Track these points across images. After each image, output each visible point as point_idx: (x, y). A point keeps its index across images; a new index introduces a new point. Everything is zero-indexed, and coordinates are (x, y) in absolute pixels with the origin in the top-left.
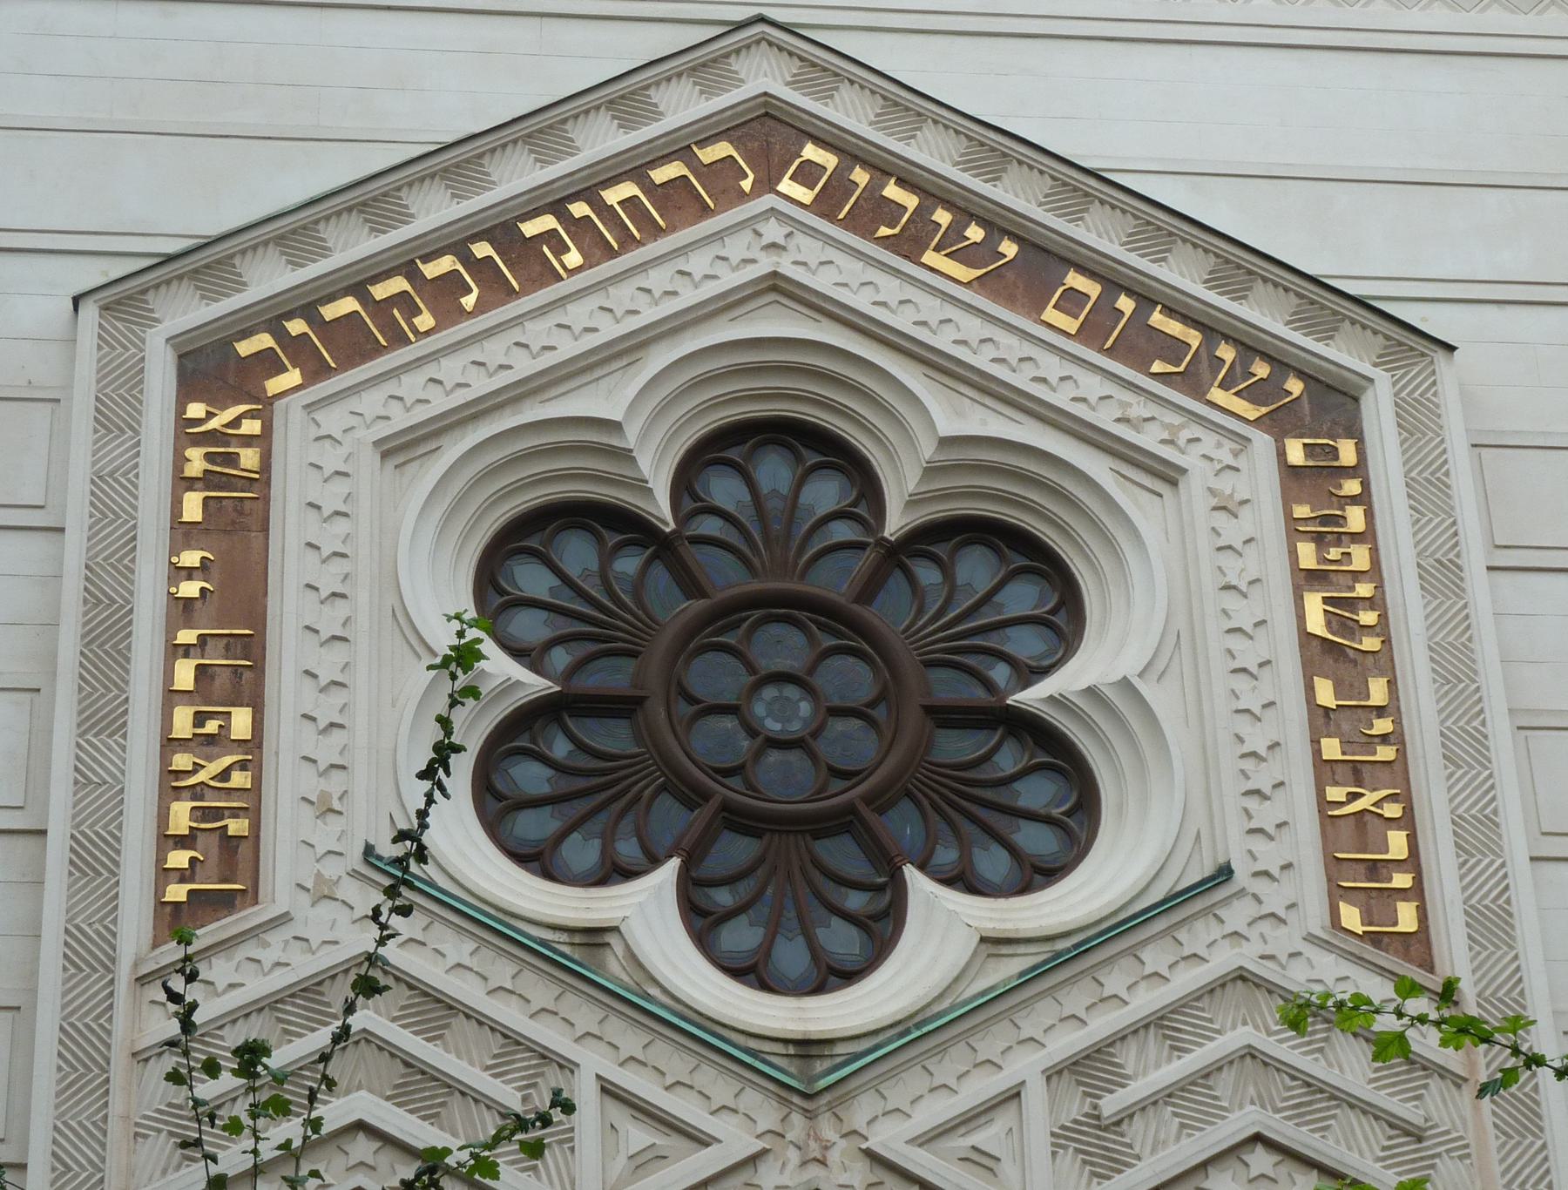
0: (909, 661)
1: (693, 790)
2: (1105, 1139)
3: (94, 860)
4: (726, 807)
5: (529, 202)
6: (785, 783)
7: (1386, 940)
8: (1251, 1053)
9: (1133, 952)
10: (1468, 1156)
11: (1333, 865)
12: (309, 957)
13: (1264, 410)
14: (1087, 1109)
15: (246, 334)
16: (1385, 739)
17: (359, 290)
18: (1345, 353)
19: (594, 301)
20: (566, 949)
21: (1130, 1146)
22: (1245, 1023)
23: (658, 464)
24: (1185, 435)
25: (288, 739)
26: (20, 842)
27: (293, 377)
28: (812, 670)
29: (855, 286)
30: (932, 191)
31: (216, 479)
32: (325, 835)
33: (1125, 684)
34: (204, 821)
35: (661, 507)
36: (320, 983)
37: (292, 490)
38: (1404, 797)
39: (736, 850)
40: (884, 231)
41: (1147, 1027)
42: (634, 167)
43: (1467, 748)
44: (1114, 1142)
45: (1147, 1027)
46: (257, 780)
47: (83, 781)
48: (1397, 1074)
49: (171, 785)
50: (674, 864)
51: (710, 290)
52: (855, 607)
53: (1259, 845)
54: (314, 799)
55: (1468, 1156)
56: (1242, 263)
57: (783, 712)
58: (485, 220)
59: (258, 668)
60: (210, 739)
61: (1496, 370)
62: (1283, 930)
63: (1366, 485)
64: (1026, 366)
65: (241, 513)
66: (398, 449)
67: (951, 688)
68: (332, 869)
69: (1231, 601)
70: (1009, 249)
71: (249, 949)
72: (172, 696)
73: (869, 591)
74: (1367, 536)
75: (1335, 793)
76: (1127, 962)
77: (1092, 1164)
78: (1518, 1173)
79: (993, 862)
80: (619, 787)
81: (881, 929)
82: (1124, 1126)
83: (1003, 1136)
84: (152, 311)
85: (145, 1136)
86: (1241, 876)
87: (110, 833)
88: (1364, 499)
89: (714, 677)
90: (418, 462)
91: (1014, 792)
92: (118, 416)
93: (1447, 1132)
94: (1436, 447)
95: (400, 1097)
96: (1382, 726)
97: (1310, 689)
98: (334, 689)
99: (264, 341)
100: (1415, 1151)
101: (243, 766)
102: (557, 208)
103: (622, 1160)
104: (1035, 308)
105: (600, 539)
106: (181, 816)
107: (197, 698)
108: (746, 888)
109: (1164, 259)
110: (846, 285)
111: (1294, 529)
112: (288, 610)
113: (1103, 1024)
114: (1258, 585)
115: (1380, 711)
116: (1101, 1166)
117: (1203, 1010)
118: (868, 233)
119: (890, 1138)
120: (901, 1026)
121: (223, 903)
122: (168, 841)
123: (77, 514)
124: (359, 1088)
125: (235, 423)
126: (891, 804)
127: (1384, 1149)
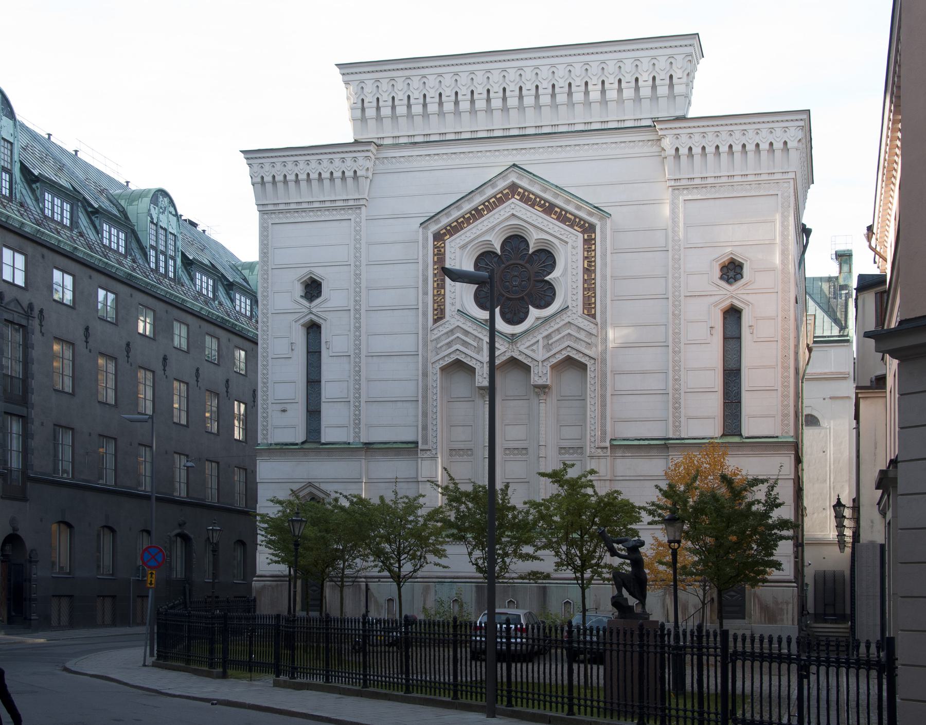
3: (425, 314)
18: (593, 220)
30: (537, 196)
32: (453, 308)
35: (499, 252)
49: (434, 303)
66: (463, 247)
72: (434, 288)
74: (595, 250)
86: (570, 307)
88: (595, 244)
91: (544, 295)
113: (550, 330)
119: (522, 348)
122: (434, 310)
123: (420, 261)
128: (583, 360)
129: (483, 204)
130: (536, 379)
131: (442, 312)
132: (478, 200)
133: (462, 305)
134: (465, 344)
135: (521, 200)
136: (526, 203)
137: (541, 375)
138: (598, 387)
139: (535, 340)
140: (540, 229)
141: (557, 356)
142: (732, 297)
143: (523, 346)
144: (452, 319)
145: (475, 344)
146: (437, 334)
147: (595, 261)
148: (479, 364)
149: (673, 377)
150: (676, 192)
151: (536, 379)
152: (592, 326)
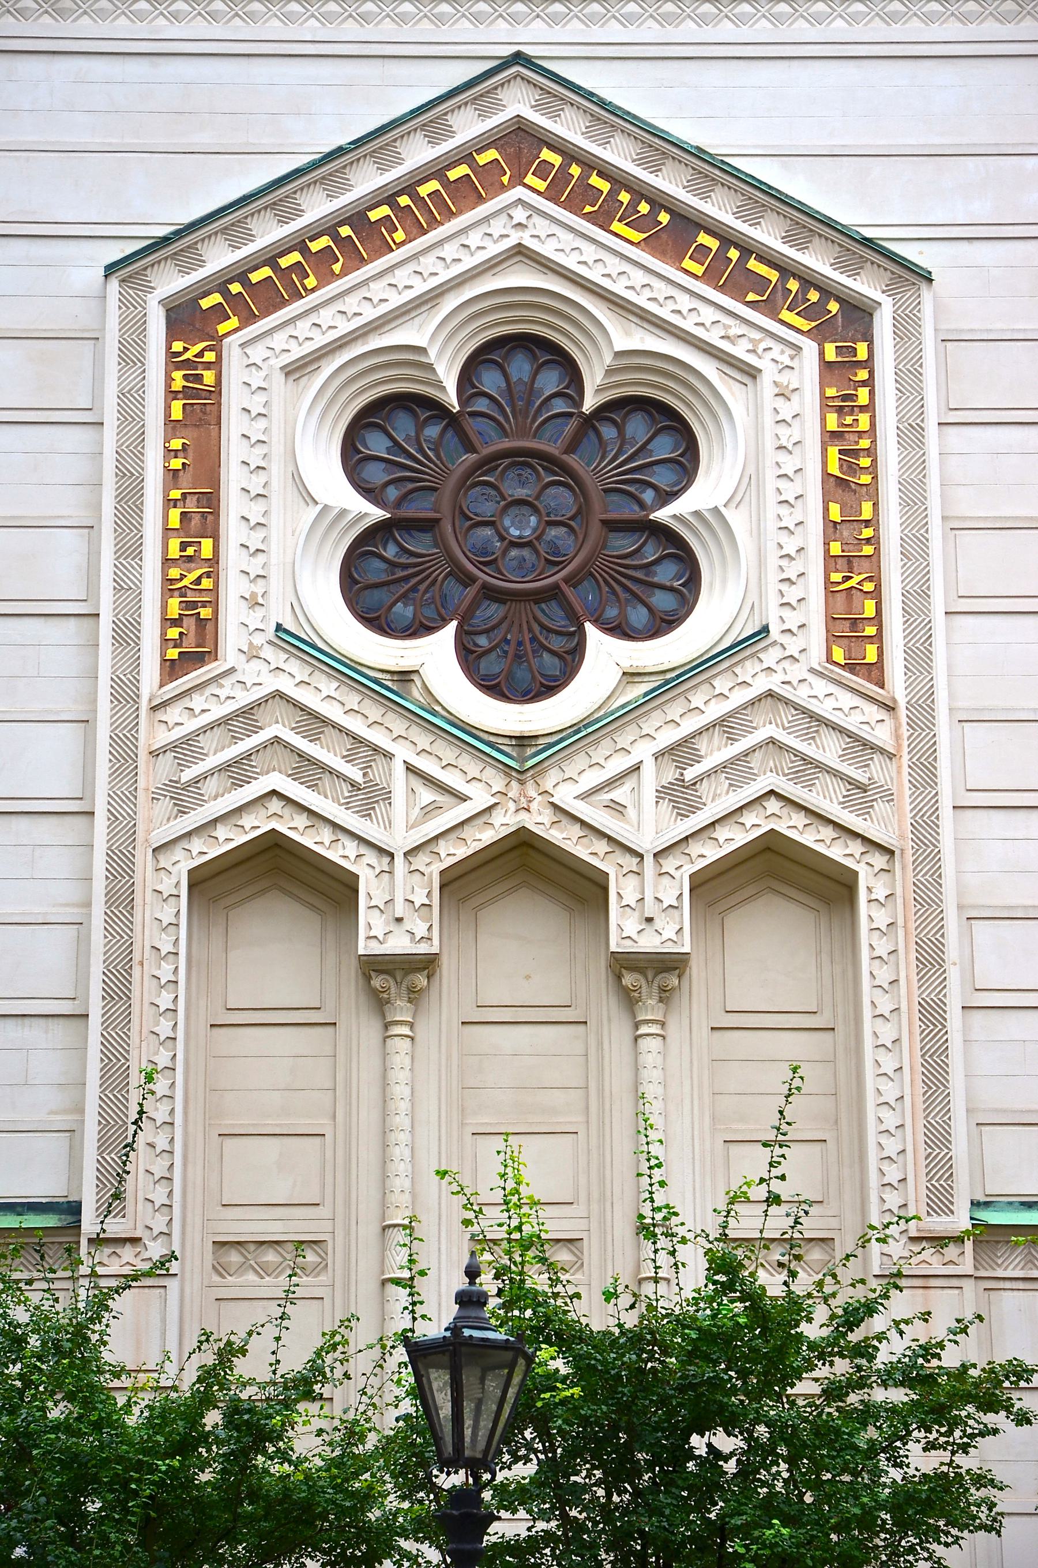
0: (594, 486)
1: (465, 575)
2: (686, 793)
3: (126, 635)
4: (485, 586)
5: (373, 198)
7: (858, 667)
8: (772, 741)
9: (708, 681)
10: (893, 800)
11: (831, 620)
12: (245, 693)
13: (814, 324)
14: (677, 776)
15: (206, 294)
16: (868, 541)
17: (272, 262)
18: (865, 286)
20: (389, 684)
21: (700, 798)
22: (771, 723)
23: (449, 369)
24: (763, 345)
25: (233, 560)
26: (86, 621)
27: (233, 322)
28: (537, 498)
29: (567, 250)
30: (618, 180)
31: (190, 391)
32: (254, 619)
33: (716, 510)
34: (187, 610)
35: (451, 398)
36: (252, 708)
37: (235, 399)
38: (876, 578)
39: (492, 611)
40: (588, 209)
41: (714, 726)
42: (437, 170)
43: (916, 547)
44: (692, 795)
45: (714, 726)
46: (216, 584)
47: (118, 588)
48: (856, 752)
49: (169, 588)
50: (454, 623)
51: (481, 257)
52: (565, 457)
53: (786, 613)
54: (248, 597)
55: (893, 800)
56: (809, 222)
58: (347, 212)
59: (216, 514)
60: (190, 559)
61: (962, 283)
62: (797, 665)
63: (871, 373)
64: (670, 302)
65: (205, 413)
68: (258, 639)
69: (782, 457)
71: (213, 689)
72: (167, 531)
73: (572, 447)
74: (869, 408)
75: (836, 577)
76: (706, 687)
77: (678, 808)
78: (920, 810)
79: (638, 616)
80: (424, 574)
81: (572, 659)
82: (698, 786)
83: (629, 792)
84: (150, 282)
85: (158, 799)
87: (134, 619)
88: (869, 383)
90: (306, 377)
92: (132, 353)
93: (882, 786)
94: (916, 347)
95: (295, 776)
96: (868, 533)
98: (258, 527)
99: (216, 298)
100: (863, 797)
101: (208, 575)
102: (390, 200)
103: (417, 810)
104: (676, 258)
105: (415, 415)
107: (182, 534)
109: (759, 223)
110: (562, 250)
111: (825, 404)
113: (690, 725)
114: (799, 445)
115: (867, 523)
116: (683, 809)
117: (747, 715)
118: (577, 211)
119: (566, 796)
120: (576, 728)
122: (168, 622)
124: (274, 770)
125: (201, 354)
126: (580, 582)
127: (844, 797)
128: (837, 852)
129: (390, 200)
131: (207, 630)
132: (367, 181)
133: (297, 607)
134: (308, 769)
135: (552, 194)
136: (572, 205)
138: (907, 969)
139: (619, 764)
140: (634, 310)
143: (569, 784)
144: (247, 666)
145: (355, 773)
146: (181, 722)
148: (371, 857)
151: (631, 925)
152: (873, 712)
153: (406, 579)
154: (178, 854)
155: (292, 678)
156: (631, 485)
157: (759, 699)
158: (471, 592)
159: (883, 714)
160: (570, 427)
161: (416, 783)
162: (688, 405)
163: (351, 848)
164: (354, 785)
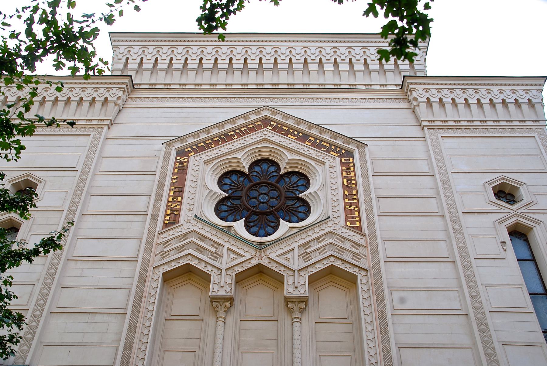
0: (283, 191)
3: (154, 218)
4: (253, 211)
6: (263, 208)
8: (331, 243)
11: (346, 217)
16: (355, 199)
18: (351, 147)
19: (238, 142)
30: (289, 128)
32: (189, 214)
35: (247, 171)
39: (255, 217)
43: (368, 200)
46: (181, 207)
47: (154, 207)
49: (168, 207)
53: (334, 213)
57: (263, 198)
59: (183, 192)
63: (354, 164)
66: (207, 162)
67: (289, 195)
69: (332, 180)
70: (301, 134)
71: (176, 229)
72: (169, 195)
73: (278, 182)
74: (354, 171)
75: (347, 207)
76: (312, 230)
79: (295, 219)
81: (276, 228)
88: (354, 166)
89: (254, 194)
96: (355, 197)
97: (344, 192)
102: (234, 131)
104: (305, 142)
106: (169, 212)
108: (256, 223)
111: (342, 170)
112: (188, 183)
113: (307, 239)
115: (355, 195)
119: (272, 256)
121: (174, 223)
122: (166, 215)
129: (234, 131)
130: (291, 290)
132: (228, 127)
137: (296, 285)
138: (374, 301)
141: (317, 266)
142: (516, 215)
143: (274, 253)
144: (186, 221)
145: (213, 250)
147: (355, 180)
148: (215, 270)
149: (470, 293)
150: (432, 130)
151: (291, 290)
152: (359, 237)
153: (232, 210)
154: (160, 269)
155: (198, 227)
156: (294, 188)
157: (327, 233)
158: (249, 212)
159: (362, 237)
160: (277, 178)
161: (229, 252)
162: (307, 172)
163: (210, 268)
164: (212, 253)
